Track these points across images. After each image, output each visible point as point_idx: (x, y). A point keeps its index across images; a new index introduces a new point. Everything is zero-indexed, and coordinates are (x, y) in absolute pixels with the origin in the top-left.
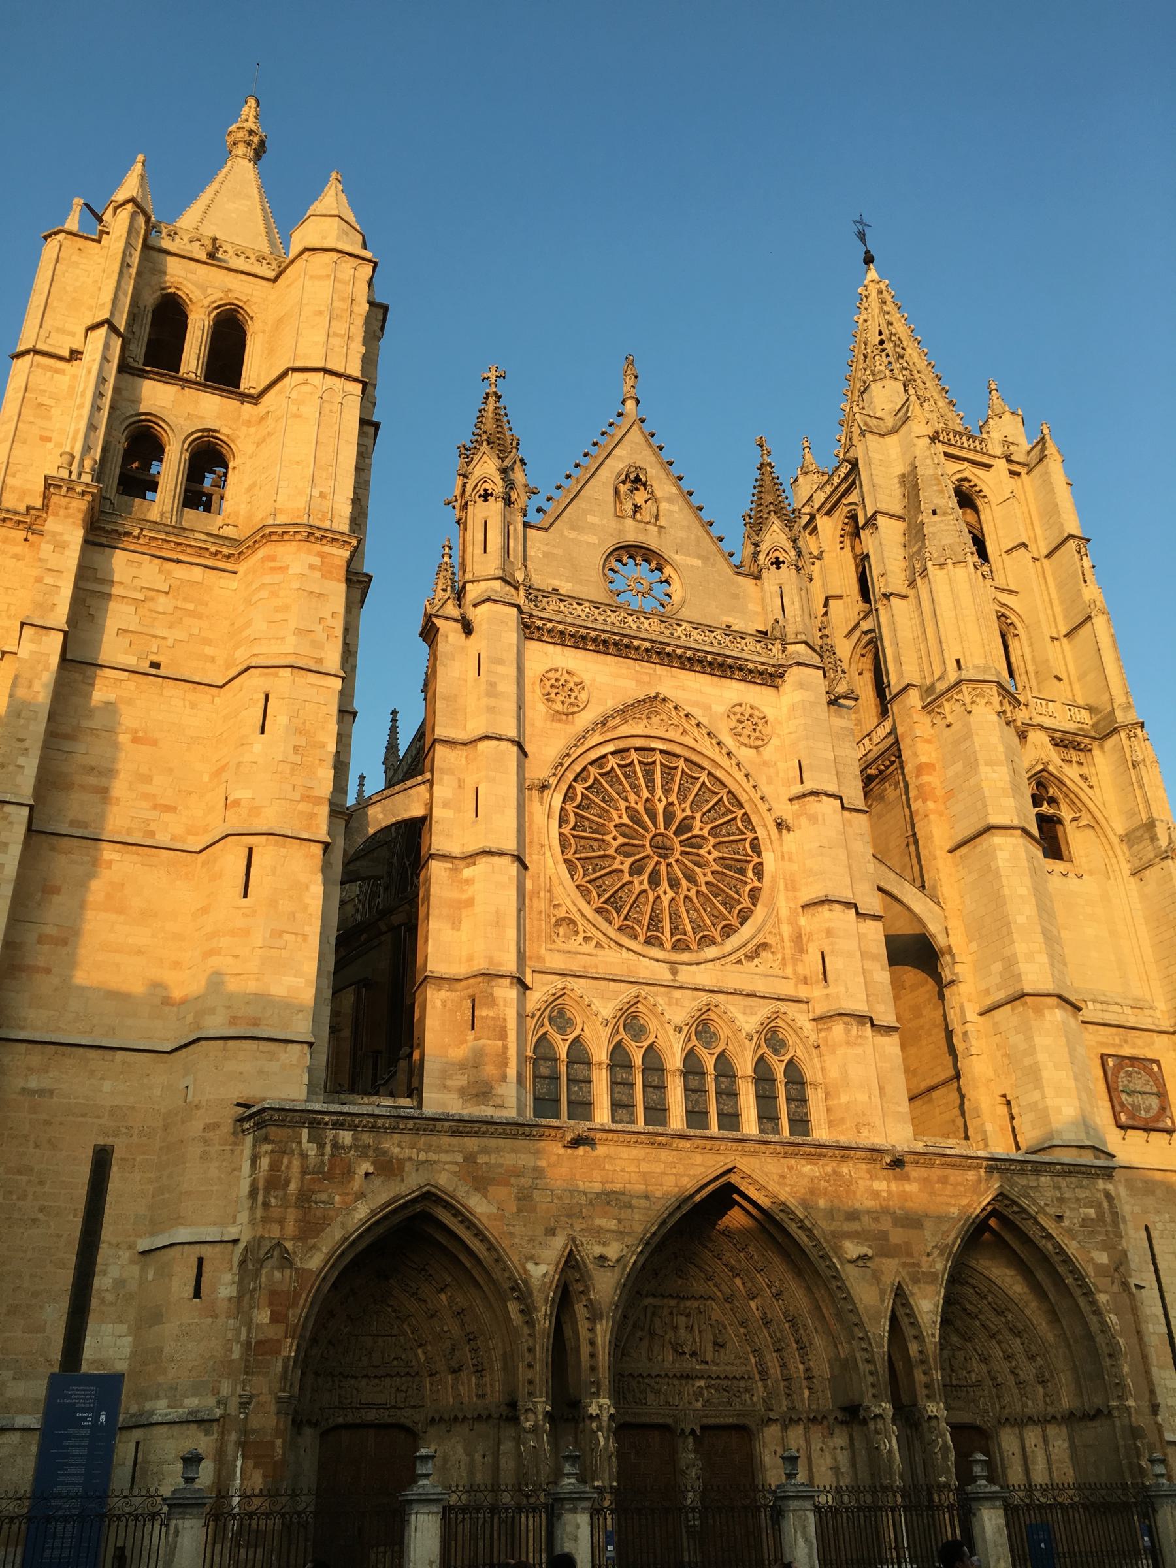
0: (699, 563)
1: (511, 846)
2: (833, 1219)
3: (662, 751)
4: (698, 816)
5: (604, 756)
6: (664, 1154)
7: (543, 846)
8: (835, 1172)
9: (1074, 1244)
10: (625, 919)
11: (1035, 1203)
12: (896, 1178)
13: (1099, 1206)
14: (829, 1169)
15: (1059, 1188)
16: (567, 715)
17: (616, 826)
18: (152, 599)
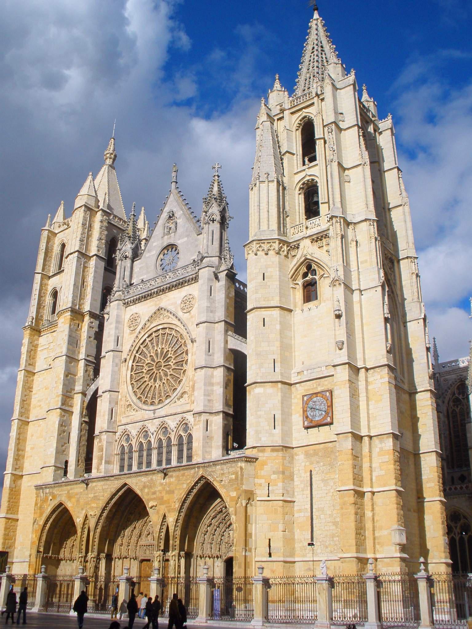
0: (186, 239)
1: (108, 388)
2: (148, 495)
3: (162, 329)
4: (170, 349)
5: (145, 340)
6: (108, 482)
7: (124, 382)
8: (151, 479)
9: (225, 490)
10: (146, 398)
11: (213, 477)
12: (168, 477)
13: (236, 473)
14: (149, 478)
15: (222, 469)
16: (134, 330)
17: (146, 365)
18: (50, 346)
